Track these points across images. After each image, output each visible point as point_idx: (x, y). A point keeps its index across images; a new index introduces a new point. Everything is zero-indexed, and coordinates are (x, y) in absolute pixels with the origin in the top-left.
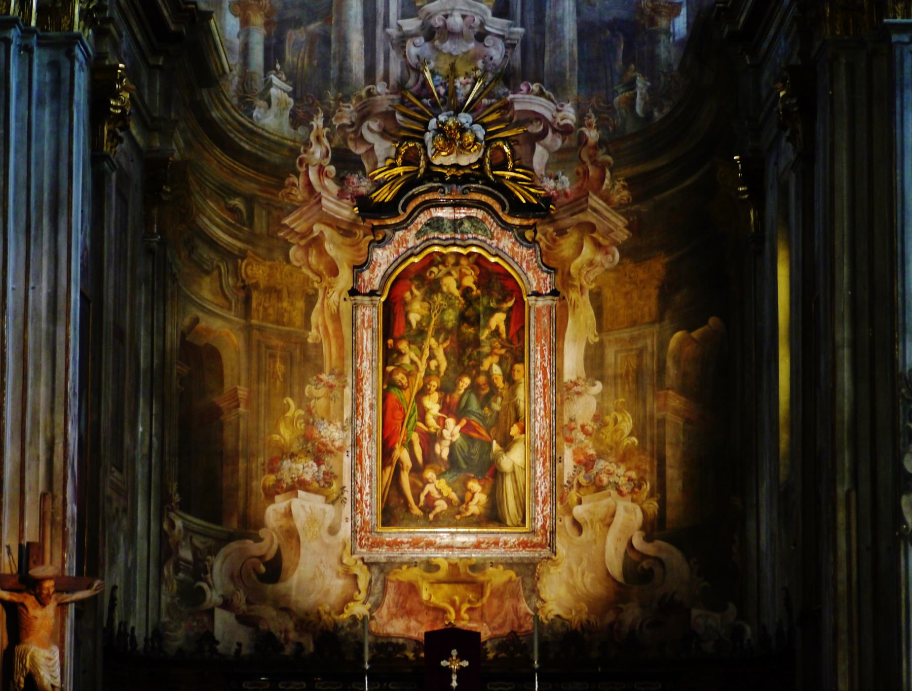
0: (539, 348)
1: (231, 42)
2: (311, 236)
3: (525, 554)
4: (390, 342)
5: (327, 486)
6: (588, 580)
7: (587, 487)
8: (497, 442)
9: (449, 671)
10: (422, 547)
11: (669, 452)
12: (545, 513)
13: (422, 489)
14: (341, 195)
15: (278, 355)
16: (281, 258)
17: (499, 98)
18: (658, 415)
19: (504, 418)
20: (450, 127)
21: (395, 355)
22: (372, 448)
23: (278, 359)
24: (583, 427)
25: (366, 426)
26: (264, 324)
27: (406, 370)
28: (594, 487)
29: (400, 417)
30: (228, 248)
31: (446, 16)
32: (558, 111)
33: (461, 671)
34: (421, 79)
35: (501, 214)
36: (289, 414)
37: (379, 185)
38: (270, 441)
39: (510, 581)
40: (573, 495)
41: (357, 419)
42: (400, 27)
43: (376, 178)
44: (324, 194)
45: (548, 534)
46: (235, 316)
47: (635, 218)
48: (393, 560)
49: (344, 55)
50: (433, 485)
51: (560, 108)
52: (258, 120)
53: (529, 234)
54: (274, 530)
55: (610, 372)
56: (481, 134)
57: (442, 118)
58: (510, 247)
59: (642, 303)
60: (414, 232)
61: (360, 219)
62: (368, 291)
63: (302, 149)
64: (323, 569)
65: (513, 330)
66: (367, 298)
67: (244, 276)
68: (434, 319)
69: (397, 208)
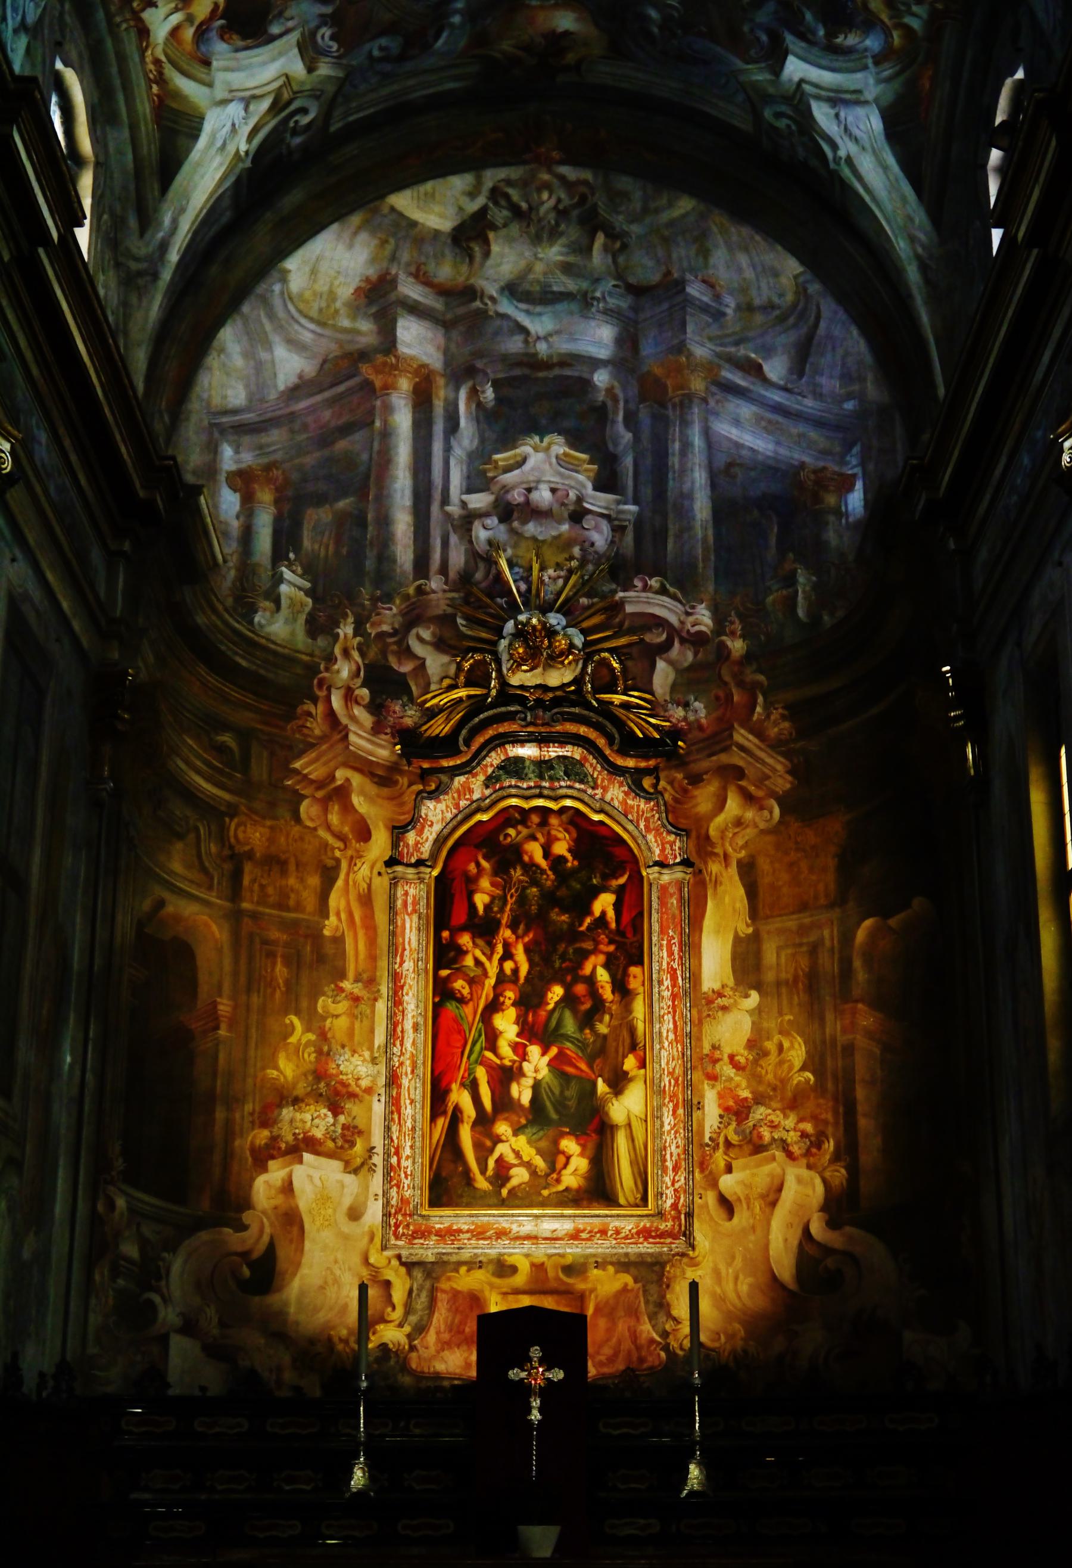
0: (665, 942)
1: (227, 524)
2: (333, 786)
3: (646, 1248)
4: (446, 934)
5: (346, 1146)
6: (744, 1288)
7: (740, 1146)
8: (604, 1081)
9: (523, 1390)
10: (490, 1238)
11: (860, 1093)
12: (677, 1185)
13: (491, 1151)
14: (377, 729)
15: (279, 954)
16: (288, 815)
17: (603, 597)
18: (842, 1039)
19: (614, 1044)
20: (534, 627)
21: (452, 954)
22: (416, 1088)
23: (279, 960)
24: (732, 1057)
25: (408, 1055)
26: (261, 909)
27: (468, 975)
28: (751, 1147)
29: (459, 1044)
30: (212, 803)
31: (529, 490)
32: (688, 614)
33: (549, 1390)
34: (493, 571)
35: (607, 752)
36: (293, 1040)
37: (431, 714)
38: (262, 1080)
39: (625, 1289)
40: (720, 1159)
41: (394, 1045)
42: (464, 504)
43: (428, 705)
44: (353, 727)
45: (683, 1216)
46: (218, 898)
47: (801, 759)
48: (445, 1258)
49: (385, 540)
50: (507, 1145)
52: (261, 626)
53: (647, 782)
54: (264, 1212)
55: (770, 976)
56: (579, 641)
57: (522, 618)
58: (621, 798)
59: (814, 877)
60: (482, 778)
61: (404, 762)
62: (413, 860)
63: (322, 667)
64: (338, 1272)
65: (626, 918)
66: (411, 870)
67: (232, 840)
68: (511, 901)
69: (458, 741)
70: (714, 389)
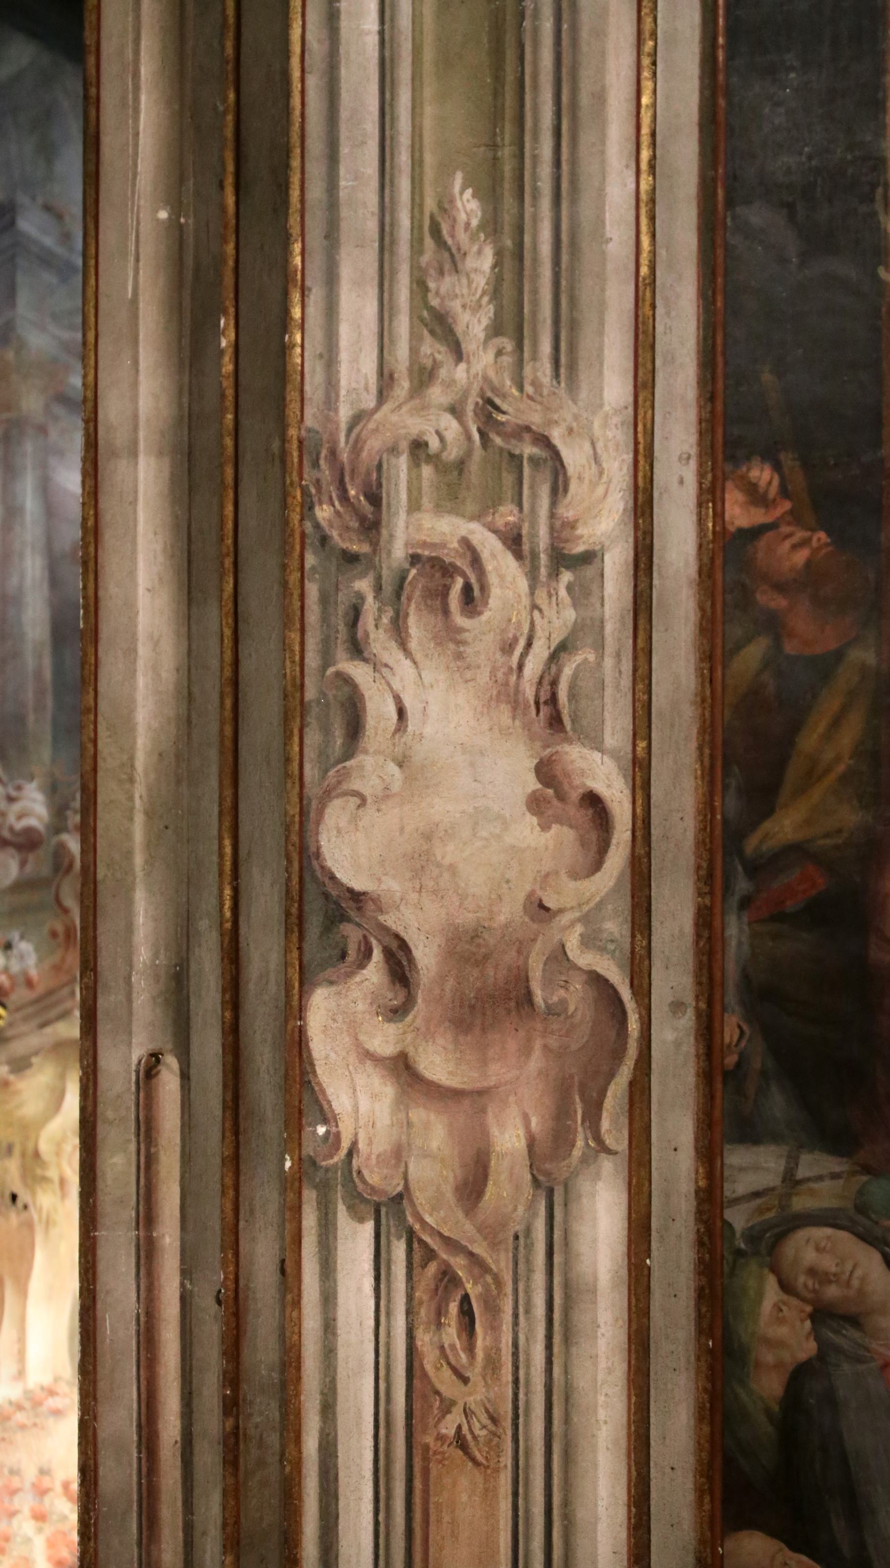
32: (11, 799)
51: (14, 793)
70: (59, 410)
